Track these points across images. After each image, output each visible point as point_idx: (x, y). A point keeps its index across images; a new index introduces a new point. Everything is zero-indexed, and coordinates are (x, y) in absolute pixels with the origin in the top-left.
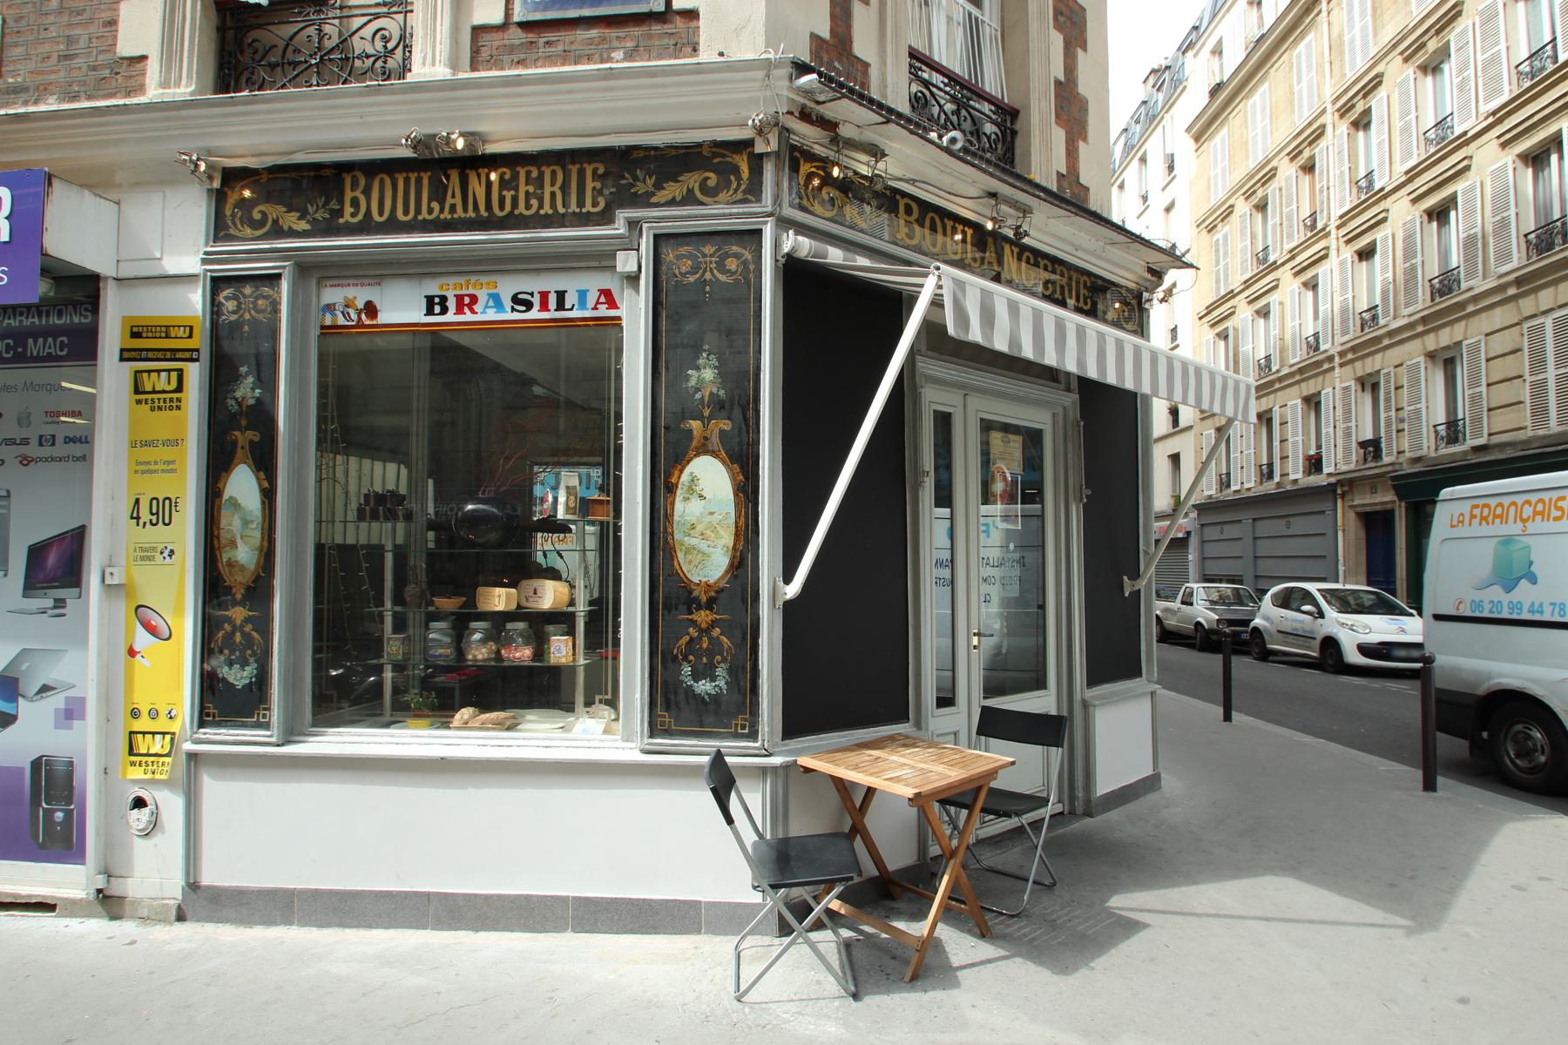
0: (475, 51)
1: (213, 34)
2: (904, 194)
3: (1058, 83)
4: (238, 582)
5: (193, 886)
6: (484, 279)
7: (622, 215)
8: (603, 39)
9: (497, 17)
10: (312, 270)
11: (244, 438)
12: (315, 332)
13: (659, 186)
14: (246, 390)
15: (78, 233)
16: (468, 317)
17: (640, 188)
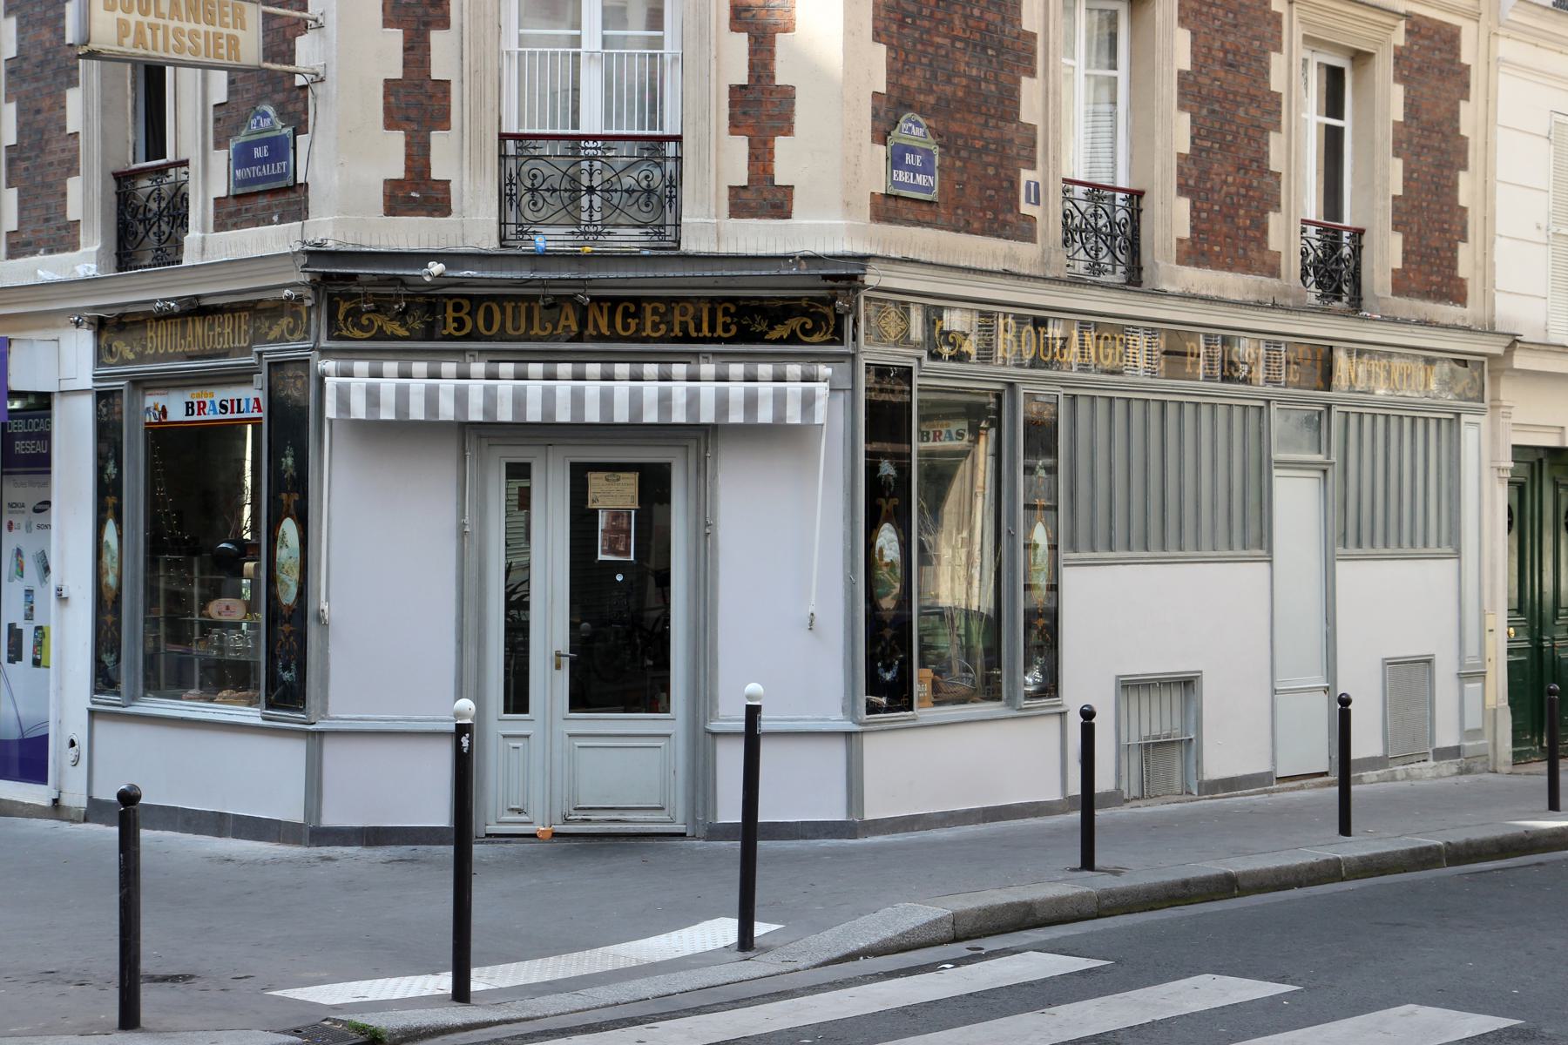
0: (217, 216)
1: (114, 199)
2: (450, 297)
3: (735, 90)
4: (109, 596)
5: (90, 798)
6: (209, 390)
7: (256, 348)
8: (270, 207)
9: (223, 193)
10: (141, 384)
11: (111, 500)
12: (142, 428)
13: (270, 328)
14: (111, 469)
15: (30, 369)
16: (202, 417)
17: (264, 330)
